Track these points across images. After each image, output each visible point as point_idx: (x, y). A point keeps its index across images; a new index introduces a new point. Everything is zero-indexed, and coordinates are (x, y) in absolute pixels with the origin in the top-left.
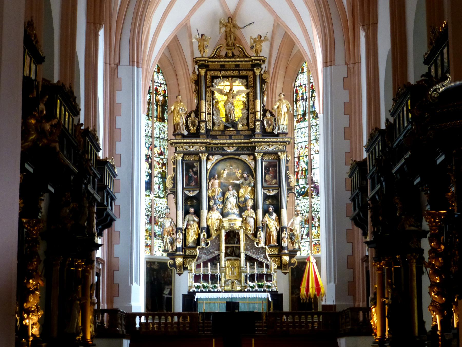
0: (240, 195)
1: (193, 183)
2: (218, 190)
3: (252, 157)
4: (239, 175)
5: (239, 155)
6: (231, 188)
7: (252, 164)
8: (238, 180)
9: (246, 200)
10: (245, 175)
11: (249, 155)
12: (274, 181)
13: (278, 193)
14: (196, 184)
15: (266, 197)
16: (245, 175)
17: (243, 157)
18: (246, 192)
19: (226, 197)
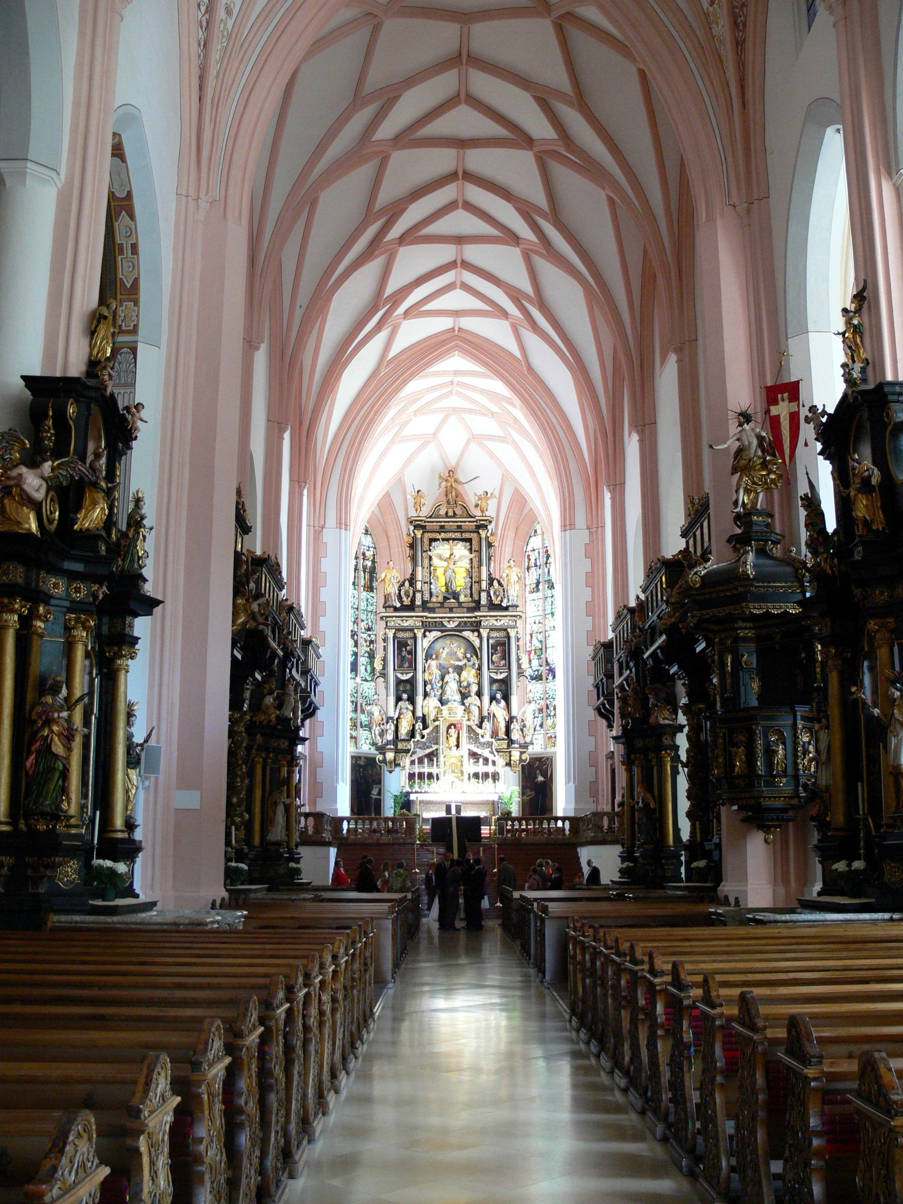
0: (462, 679)
1: (406, 665)
2: (437, 673)
3: (476, 634)
4: (460, 655)
5: (461, 631)
6: (451, 670)
7: (477, 643)
8: (460, 660)
9: (469, 685)
10: (468, 655)
11: (473, 631)
12: (503, 662)
13: (507, 677)
14: (410, 666)
15: (493, 681)
16: (468, 655)
17: (466, 634)
18: (469, 675)
19: (445, 680)
